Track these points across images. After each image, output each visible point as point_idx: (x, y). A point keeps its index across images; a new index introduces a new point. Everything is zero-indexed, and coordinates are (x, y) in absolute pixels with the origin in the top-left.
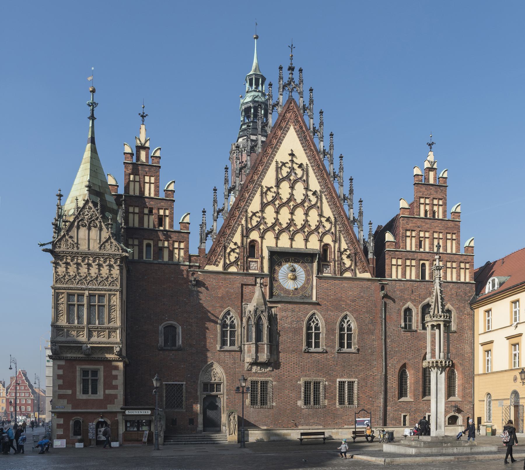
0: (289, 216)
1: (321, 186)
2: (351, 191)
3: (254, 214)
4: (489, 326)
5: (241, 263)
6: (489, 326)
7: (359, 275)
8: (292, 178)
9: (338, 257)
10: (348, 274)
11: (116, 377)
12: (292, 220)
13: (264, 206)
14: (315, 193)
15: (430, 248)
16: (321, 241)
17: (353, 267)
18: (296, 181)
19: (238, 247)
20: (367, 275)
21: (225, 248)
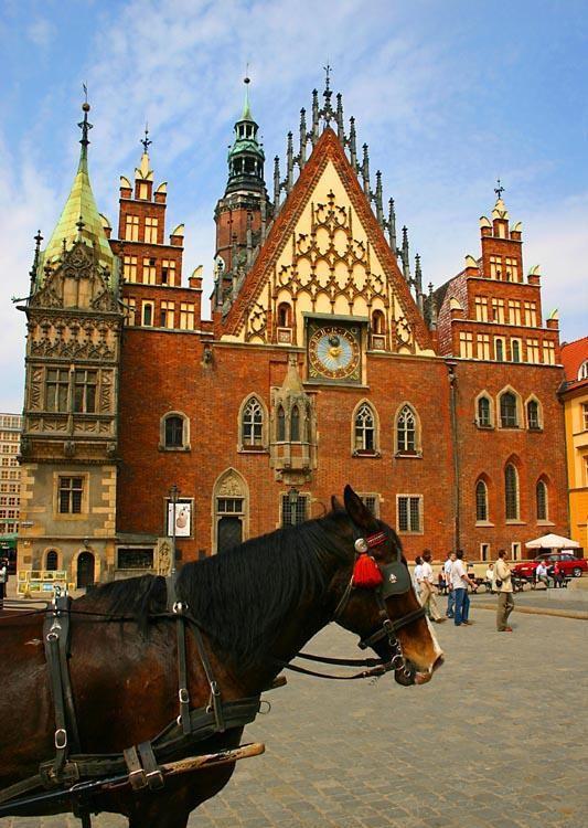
0: (330, 273)
2: (405, 245)
3: (285, 269)
5: (269, 332)
7: (419, 352)
8: (332, 225)
10: (404, 351)
11: (106, 489)
12: (332, 278)
13: (297, 258)
14: (360, 245)
15: (507, 320)
16: (369, 306)
17: (411, 342)
18: (336, 229)
19: (265, 312)
20: (430, 353)
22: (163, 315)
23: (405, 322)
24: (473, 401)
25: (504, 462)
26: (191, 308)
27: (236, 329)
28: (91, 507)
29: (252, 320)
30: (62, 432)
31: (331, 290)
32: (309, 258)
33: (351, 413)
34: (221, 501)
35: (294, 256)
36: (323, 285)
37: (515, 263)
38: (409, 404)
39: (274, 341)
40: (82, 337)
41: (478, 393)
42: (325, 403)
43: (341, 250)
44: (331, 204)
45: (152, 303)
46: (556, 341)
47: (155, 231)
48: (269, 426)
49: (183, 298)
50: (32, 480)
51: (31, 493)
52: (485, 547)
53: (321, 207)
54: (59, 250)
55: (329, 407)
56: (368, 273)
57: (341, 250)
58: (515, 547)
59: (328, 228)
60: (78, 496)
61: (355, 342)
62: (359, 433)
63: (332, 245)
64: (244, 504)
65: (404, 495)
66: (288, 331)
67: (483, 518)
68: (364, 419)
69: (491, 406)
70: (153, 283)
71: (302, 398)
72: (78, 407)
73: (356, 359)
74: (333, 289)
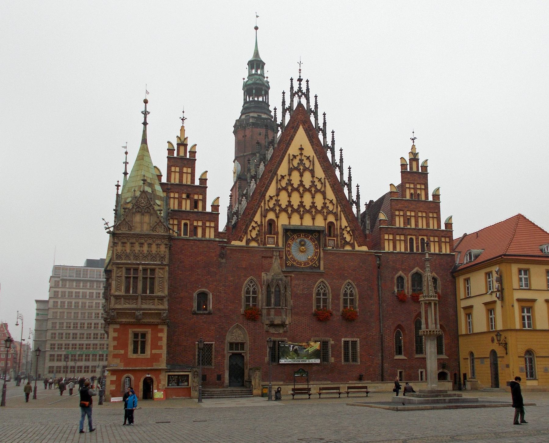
1: (325, 174)
3: (271, 198)
4: (468, 293)
6: (468, 293)
7: (357, 248)
8: (302, 168)
9: (341, 233)
10: (348, 248)
11: (161, 339)
12: (302, 202)
13: (279, 191)
14: (320, 180)
15: (416, 225)
16: (325, 219)
17: (352, 241)
19: (259, 226)
20: (364, 248)
21: (247, 227)
22: (196, 228)
23: (348, 229)
24: (393, 278)
25: (413, 318)
26: (212, 224)
27: (241, 237)
28: (152, 349)
29: (251, 231)
31: (301, 210)
32: (287, 190)
34: (231, 344)
35: (277, 189)
36: (296, 207)
37: (423, 187)
38: (350, 281)
39: (265, 244)
40: (145, 248)
41: (396, 273)
42: (296, 282)
43: (307, 184)
44: (301, 154)
45: (188, 222)
46: (451, 237)
47: (189, 176)
48: (261, 297)
49: (208, 218)
50: (116, 335)
51: (116, 342)
52: (401, 373)
53: (295, 157)
54: (130, 194)
56: (325, 198)
57: (307, 184)
58: (421, 372)
59: (299, 170)
60: (143, 344)
61: (316, 242)
62: (318, 300)
63: (301, 181)
64: (245, 346)
65: (347, 339)
67: (400, 353)
68: (322, 291)
69: (405, 281)
70: (188, 209)
71: (281, 280)
72: (144, 291)
74: (302, 209)
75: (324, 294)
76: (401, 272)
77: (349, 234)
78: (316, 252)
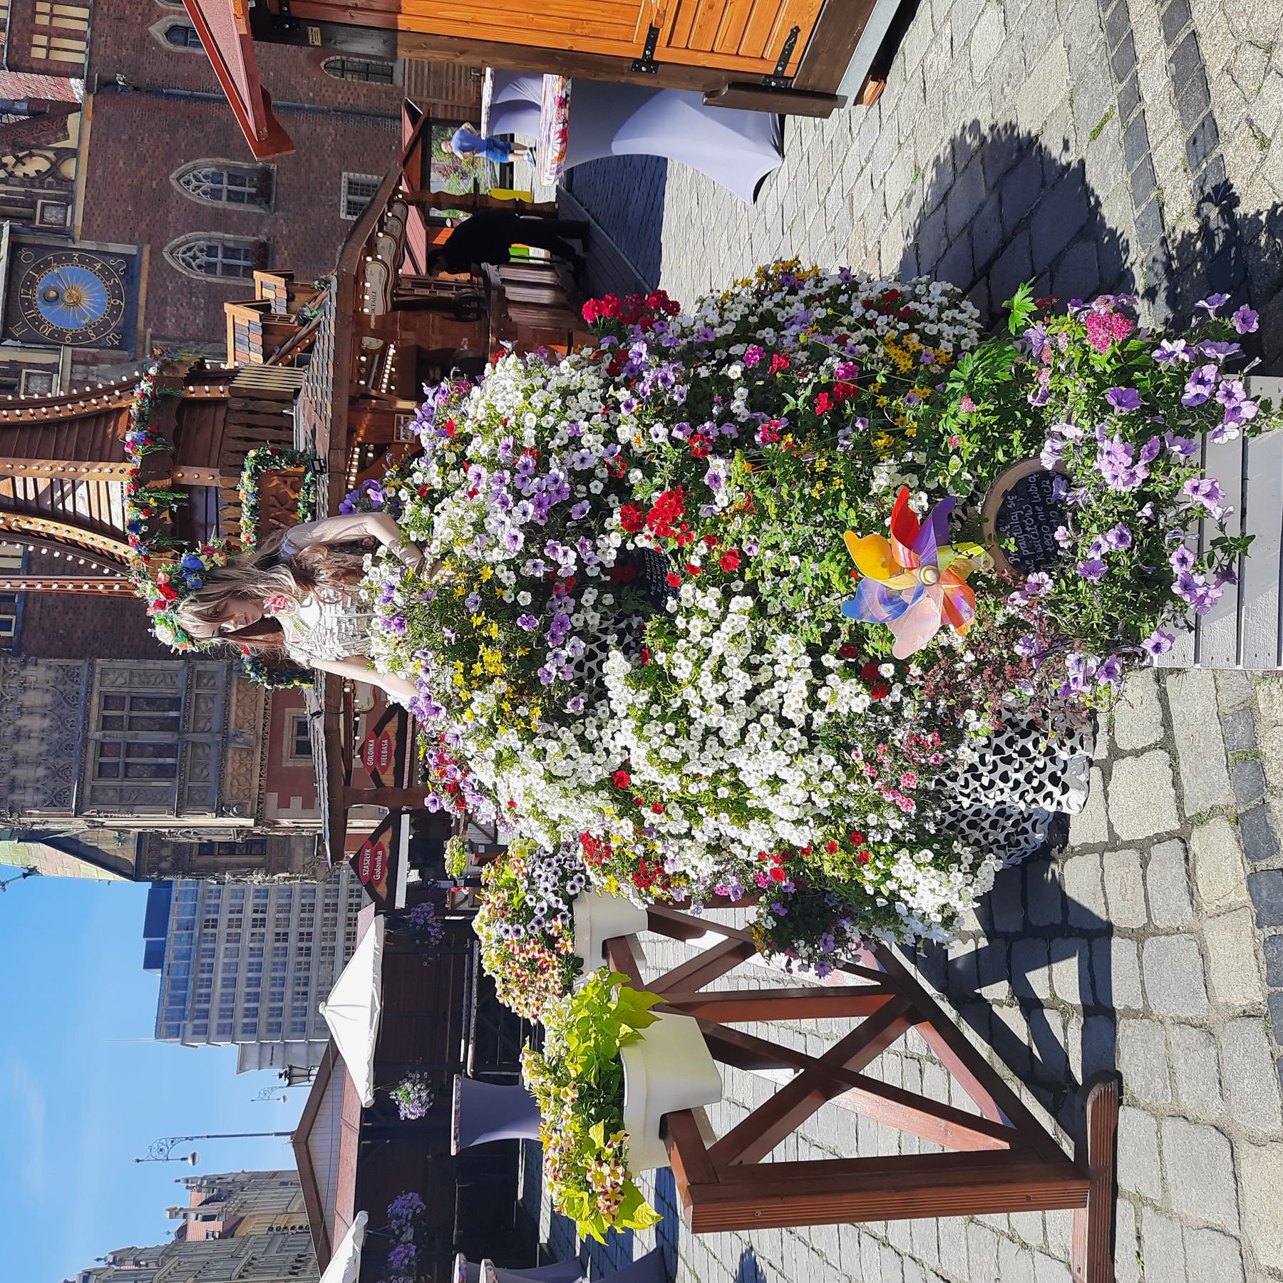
9: (22, 184)
24: (168, 54)
30: (213, 753)
33: (190, 280)
41: (157, 44)
42: (170, 323)
55: (179, 317)
65: (343, 204)
66: (28, 375)
68: (203, 259)
73: (86, 258)
75: (211, 251)
76: (152, 29)
77: (26, 160)
78: (82, 260)
